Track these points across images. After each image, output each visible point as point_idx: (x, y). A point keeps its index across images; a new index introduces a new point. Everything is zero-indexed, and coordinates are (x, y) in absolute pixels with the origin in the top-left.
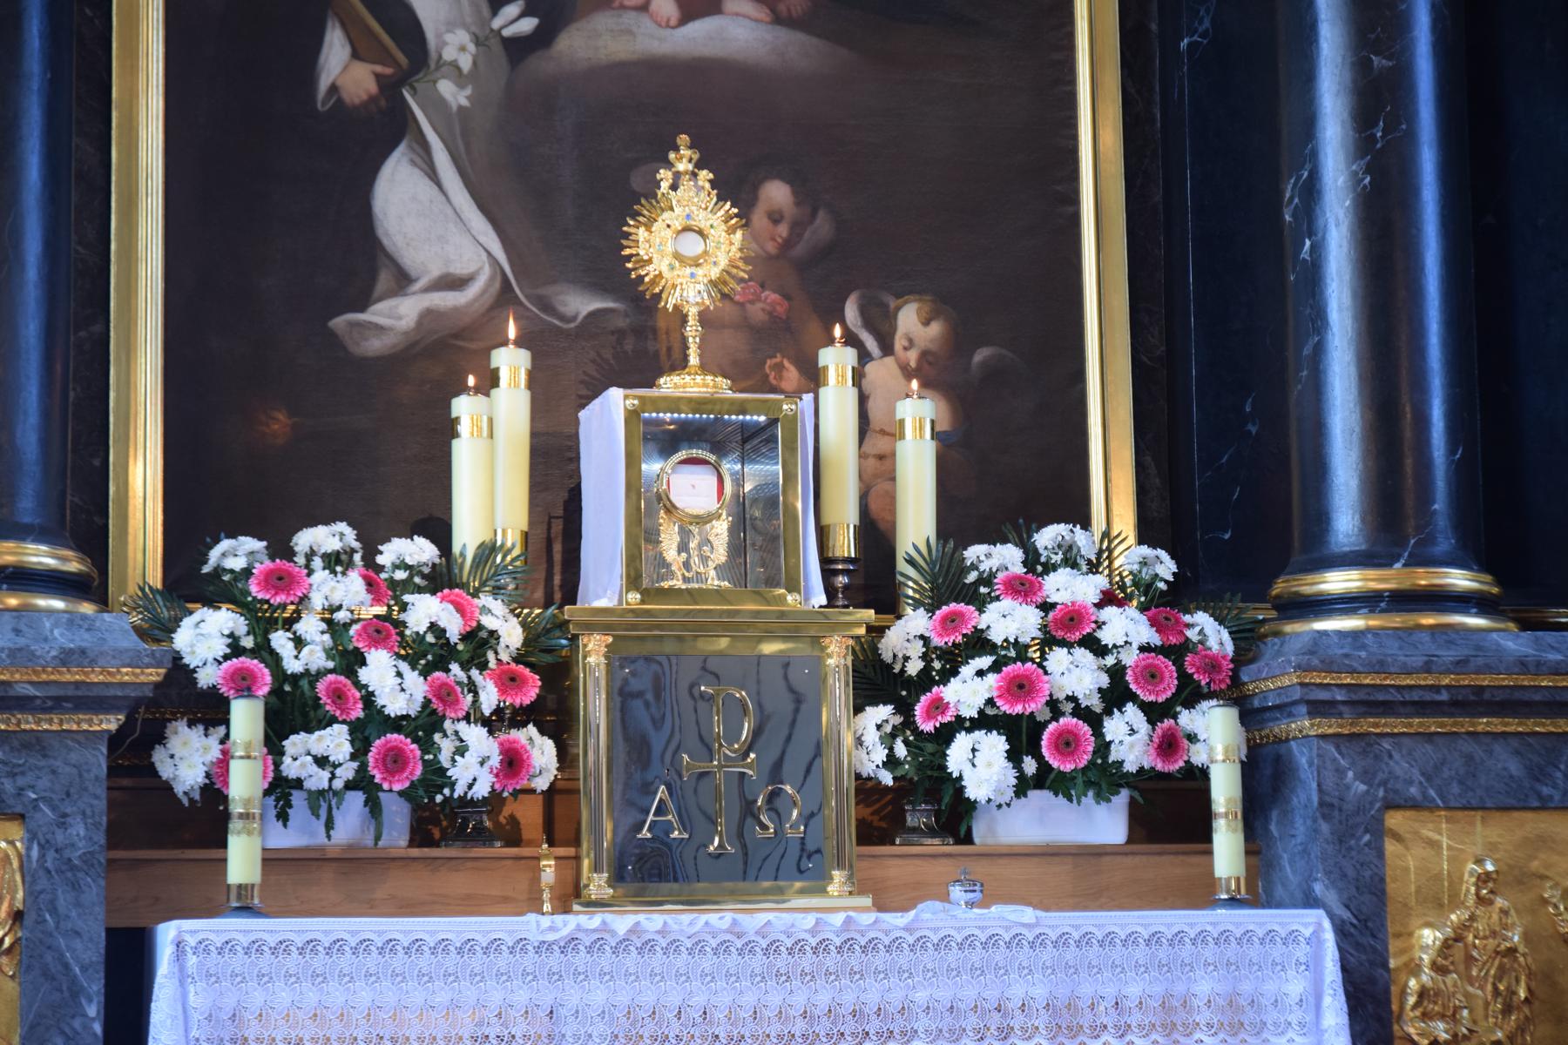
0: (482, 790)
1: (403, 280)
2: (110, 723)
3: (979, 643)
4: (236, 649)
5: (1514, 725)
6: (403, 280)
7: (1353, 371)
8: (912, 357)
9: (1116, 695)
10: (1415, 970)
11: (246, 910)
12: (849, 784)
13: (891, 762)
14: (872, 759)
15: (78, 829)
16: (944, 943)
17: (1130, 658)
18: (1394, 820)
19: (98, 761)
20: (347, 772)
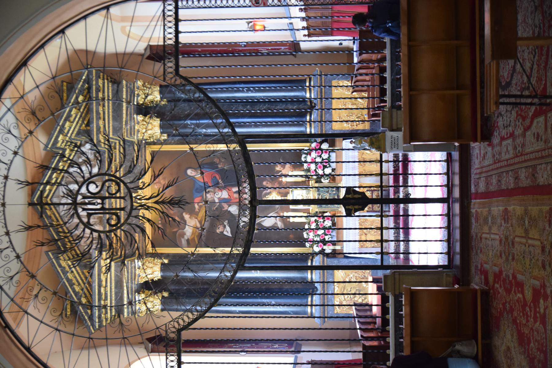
0: (331, 222)
2: (325, 259)
3: (315, 170)
4: (318, 246)
5: (324, 115)
6: (276, 223)
8: (282, 168)
9: (320, 156)
10: (349, 126)
11: (343, 247)
12: (329, 184)
13: (327, 179)
14: (327, 181)
15: (335, 262)
16: (346, 181)
17: (317, 155)
18: (333, 128)
19: (329, 260)
20: (330, 236)
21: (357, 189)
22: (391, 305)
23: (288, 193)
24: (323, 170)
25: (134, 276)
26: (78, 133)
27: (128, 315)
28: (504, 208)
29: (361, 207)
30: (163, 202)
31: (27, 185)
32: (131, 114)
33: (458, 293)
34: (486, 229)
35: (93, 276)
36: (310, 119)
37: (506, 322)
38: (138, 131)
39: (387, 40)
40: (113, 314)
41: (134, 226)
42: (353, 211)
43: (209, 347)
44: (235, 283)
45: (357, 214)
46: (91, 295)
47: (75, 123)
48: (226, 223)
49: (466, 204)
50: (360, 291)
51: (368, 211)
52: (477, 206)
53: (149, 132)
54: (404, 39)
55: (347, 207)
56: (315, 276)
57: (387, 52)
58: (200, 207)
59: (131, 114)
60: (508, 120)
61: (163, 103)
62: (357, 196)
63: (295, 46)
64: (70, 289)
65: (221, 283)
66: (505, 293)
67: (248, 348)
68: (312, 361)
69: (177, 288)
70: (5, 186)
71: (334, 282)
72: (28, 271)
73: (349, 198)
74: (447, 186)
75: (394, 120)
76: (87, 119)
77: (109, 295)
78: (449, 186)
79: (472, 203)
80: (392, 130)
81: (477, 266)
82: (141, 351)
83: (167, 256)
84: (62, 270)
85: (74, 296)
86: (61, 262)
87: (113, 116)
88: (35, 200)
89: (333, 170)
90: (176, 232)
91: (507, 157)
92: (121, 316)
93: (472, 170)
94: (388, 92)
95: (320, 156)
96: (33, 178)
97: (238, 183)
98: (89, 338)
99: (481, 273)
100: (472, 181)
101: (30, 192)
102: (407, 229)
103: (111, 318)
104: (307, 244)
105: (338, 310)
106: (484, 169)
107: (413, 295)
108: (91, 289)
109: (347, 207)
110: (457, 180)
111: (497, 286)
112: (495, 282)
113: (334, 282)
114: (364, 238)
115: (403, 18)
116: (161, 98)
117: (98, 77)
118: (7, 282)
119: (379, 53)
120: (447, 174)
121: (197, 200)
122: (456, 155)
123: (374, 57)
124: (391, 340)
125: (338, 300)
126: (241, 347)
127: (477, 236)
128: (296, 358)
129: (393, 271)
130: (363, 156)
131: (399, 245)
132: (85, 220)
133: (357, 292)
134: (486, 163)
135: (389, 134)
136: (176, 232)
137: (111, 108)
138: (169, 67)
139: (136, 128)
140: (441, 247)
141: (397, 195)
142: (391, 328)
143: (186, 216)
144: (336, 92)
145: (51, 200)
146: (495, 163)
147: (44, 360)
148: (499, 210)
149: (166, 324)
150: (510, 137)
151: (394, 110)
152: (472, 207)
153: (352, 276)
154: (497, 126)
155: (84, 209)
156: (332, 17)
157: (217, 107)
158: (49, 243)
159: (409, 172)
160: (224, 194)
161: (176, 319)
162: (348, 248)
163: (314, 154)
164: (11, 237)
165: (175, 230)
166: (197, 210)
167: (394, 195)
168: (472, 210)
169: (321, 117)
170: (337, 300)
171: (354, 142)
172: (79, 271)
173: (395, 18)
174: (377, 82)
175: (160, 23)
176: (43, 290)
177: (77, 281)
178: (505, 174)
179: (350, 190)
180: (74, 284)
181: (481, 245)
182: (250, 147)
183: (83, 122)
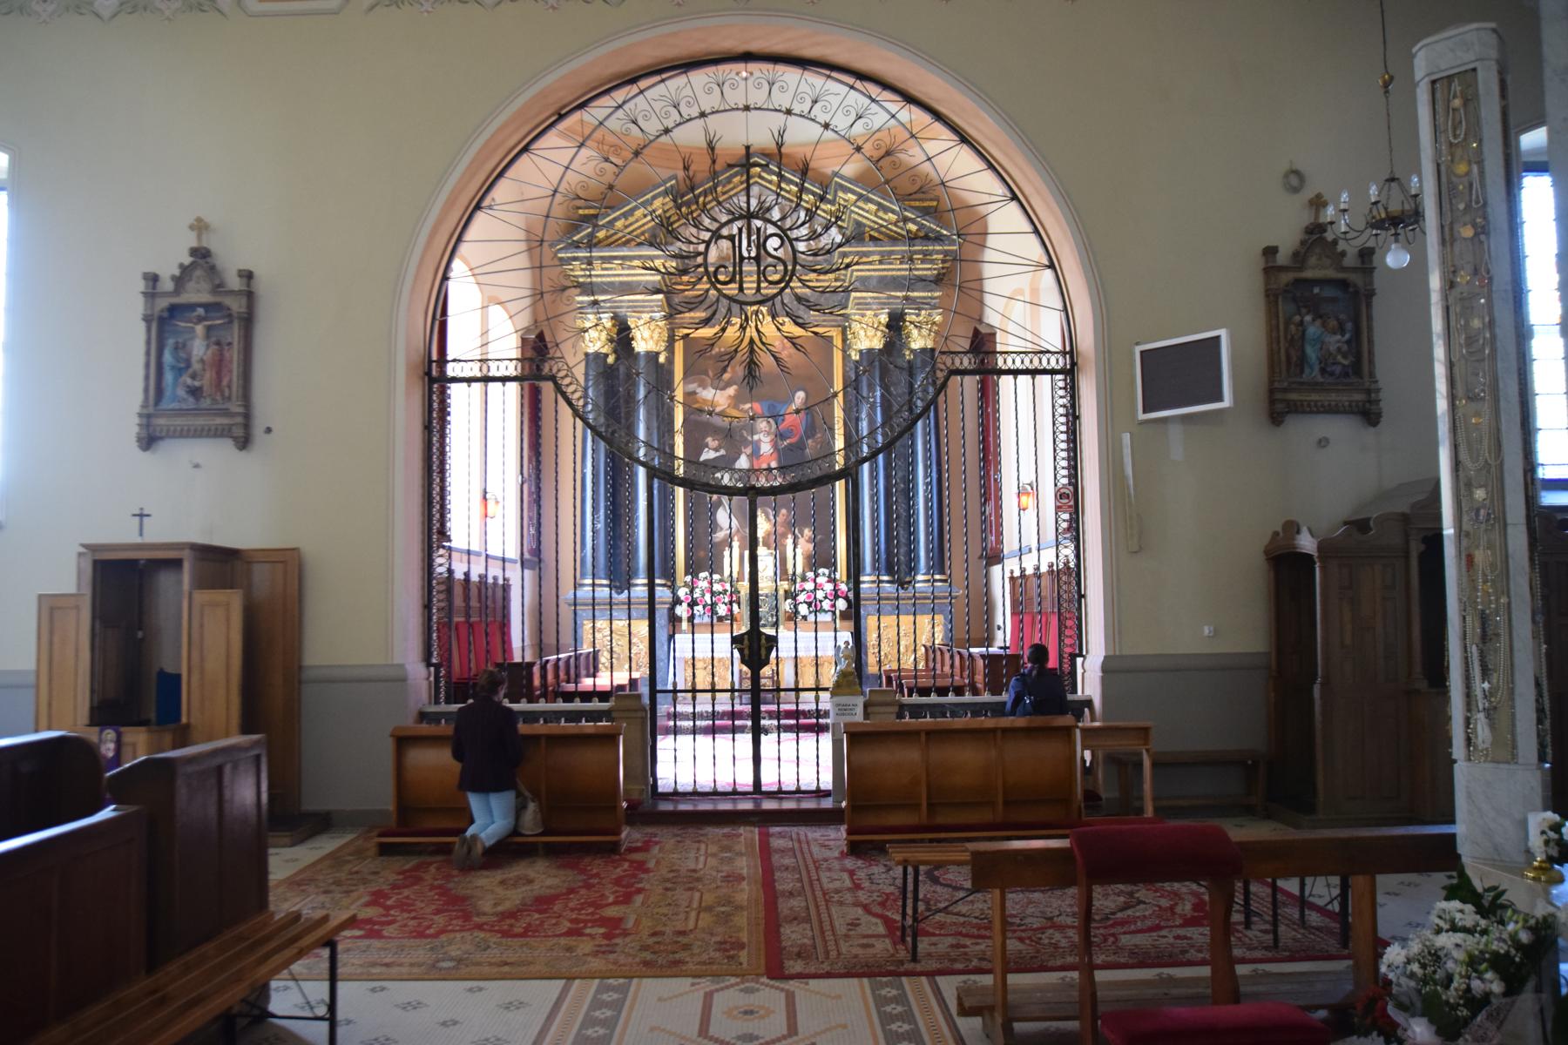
1: (722, 529)
2: (667, 606)
3: (804, 590)
6: (722, 529)
7: (864, 541)
9: (826, 598)
14: (788, 609)
19: (666, 611)
21: (773, 654)
22: (596, 705)
23: (769, 549)
24: (805, 602)
25: (637, 309)
26: (859, 224)
27: (579, 303)
28: (745, 875)
29: (746, 658)
30: (752, 351)
31: (777, 144)
32: (889, 304)
33: (615, 808)
34: (713, 849)
35: (638, 248)
36: (883, 582)
37: (570, 878)
38: (863, 316)
39: (1005, 697)
40: (581, 280)
41: (714, 307)
42: (739, 646)
43: (530, 428)
44: (628, 464)
45: (736, 652)
46: (609, 245)
47: (875, 219)
48: (722, 452)
49: (752, 819)
50: (618, 659)
51: (741, 671)
52: (749, 835)
53: (862, 333)
54: (1006, 722)
55: (746, 636)
56: (640, 590)
57: (986, 697)
58: (747, 411)
59: (889, 304)
60: (881, 881)
61: (907, 353)
62: (763, 652)
63: (995, 557)
64: (618, 213)
65: (628, 442)
66: (614, 877)
67: (530, 489)
68: (509, 586)
69: (621, 377)
70: (776, 110)
71: (630, 619)
72: (645, 146)
73: (760, 640)
74: (780, 791)
75: (882, 709)
76: (881, 237)
77: (610, 272)
78: (779, 794)
79: (752, 828)
80: (866, 706)
81: (655, 835)
82: (524, 320)
83: (670, 360)
84: (648, 200)
85: (608, 219)
86: (661, 199)
87: (886, 276)
88: (756, 159)
89: (805, 618)
90: (708, 376)
91: (824, 880)
92: (578, 291)
93: (803, 828)
94: (924, 700)
95: (826, 598)
96: (788, 156)
97: (782, 468)
98: (542, 241)
99: (646, 842)
100: (787, 829)
101: (767, 152)
102: (713, 731)
103: (574, 276)
104: (689, 578)
105: (588, 625)
106: (805, 846)
107: (610, 739)
108: (619, 245)
109: (746, 636)
110: (789, 805)
111: (626, 865)
112: (632, 862)
113: (630, 619)
114: (699, 665)
115: (1039, 721)
116: (913, 351)
117: (946, 253)
118: (628, 116)
119: (985, 685)
120: (798, 791)
121: (757, 406)
122: (827, 803)
123: (979, 678)
124: (542, 706)
125: (604, 626)
126: (530, 476)
127: (702, 835)
128: (514, 562)
129: (648, 708)
130: (826, 664)
131: (689, 720)
132: (725, 232)
133: (614, 656)
134: (815, 849)
135: (860, 701)
136: (708, 376)
137: (899, 273)
138: (961, 360)
139: (869, 313)
140: (685, 783)
141: (766, 715)
142: (560, 705)
143: (731, 391)
144: (924, 621)
145: (756, 182)
146: (814, 862)
147: (510, 173)
148: (742, 869)
149: (563, 358)
150: (854, 883)
151: (896, 709)
152: (748, 828)
153: (641, 647)
154: (871, 865)
155: (740, 230)
156: (1040, 612)
157: (901, 435)
158: (688, 177)
159: (800, 735)
160: (766, 448)
161: (572, 373)
162: (683, 640)
163: (829, 587)
164: (697, 120)
165: (711, 374)
166: (742, 406)
167: (766, 712)
168: (742, 828)
169: (887, 599)
170: (602, 624)
171: (847, 647)
172: (646, 227)
173: (1039, 708)
174: (940, 683)
175: (1030, 347)
176: (616, 170)
177: (631, 224)
178: (798, 876)
179: (773, 641)
180: (626, 219)
181: (688, 842)
182: (840, 486)
183: (877, 230)
